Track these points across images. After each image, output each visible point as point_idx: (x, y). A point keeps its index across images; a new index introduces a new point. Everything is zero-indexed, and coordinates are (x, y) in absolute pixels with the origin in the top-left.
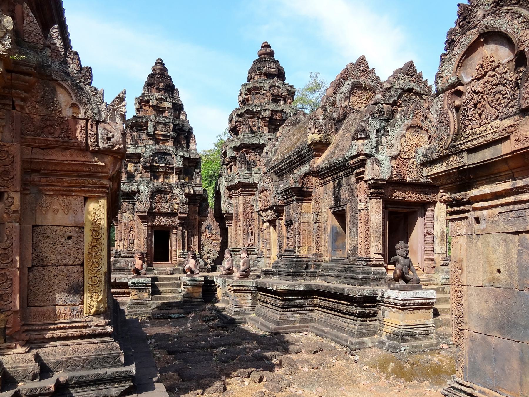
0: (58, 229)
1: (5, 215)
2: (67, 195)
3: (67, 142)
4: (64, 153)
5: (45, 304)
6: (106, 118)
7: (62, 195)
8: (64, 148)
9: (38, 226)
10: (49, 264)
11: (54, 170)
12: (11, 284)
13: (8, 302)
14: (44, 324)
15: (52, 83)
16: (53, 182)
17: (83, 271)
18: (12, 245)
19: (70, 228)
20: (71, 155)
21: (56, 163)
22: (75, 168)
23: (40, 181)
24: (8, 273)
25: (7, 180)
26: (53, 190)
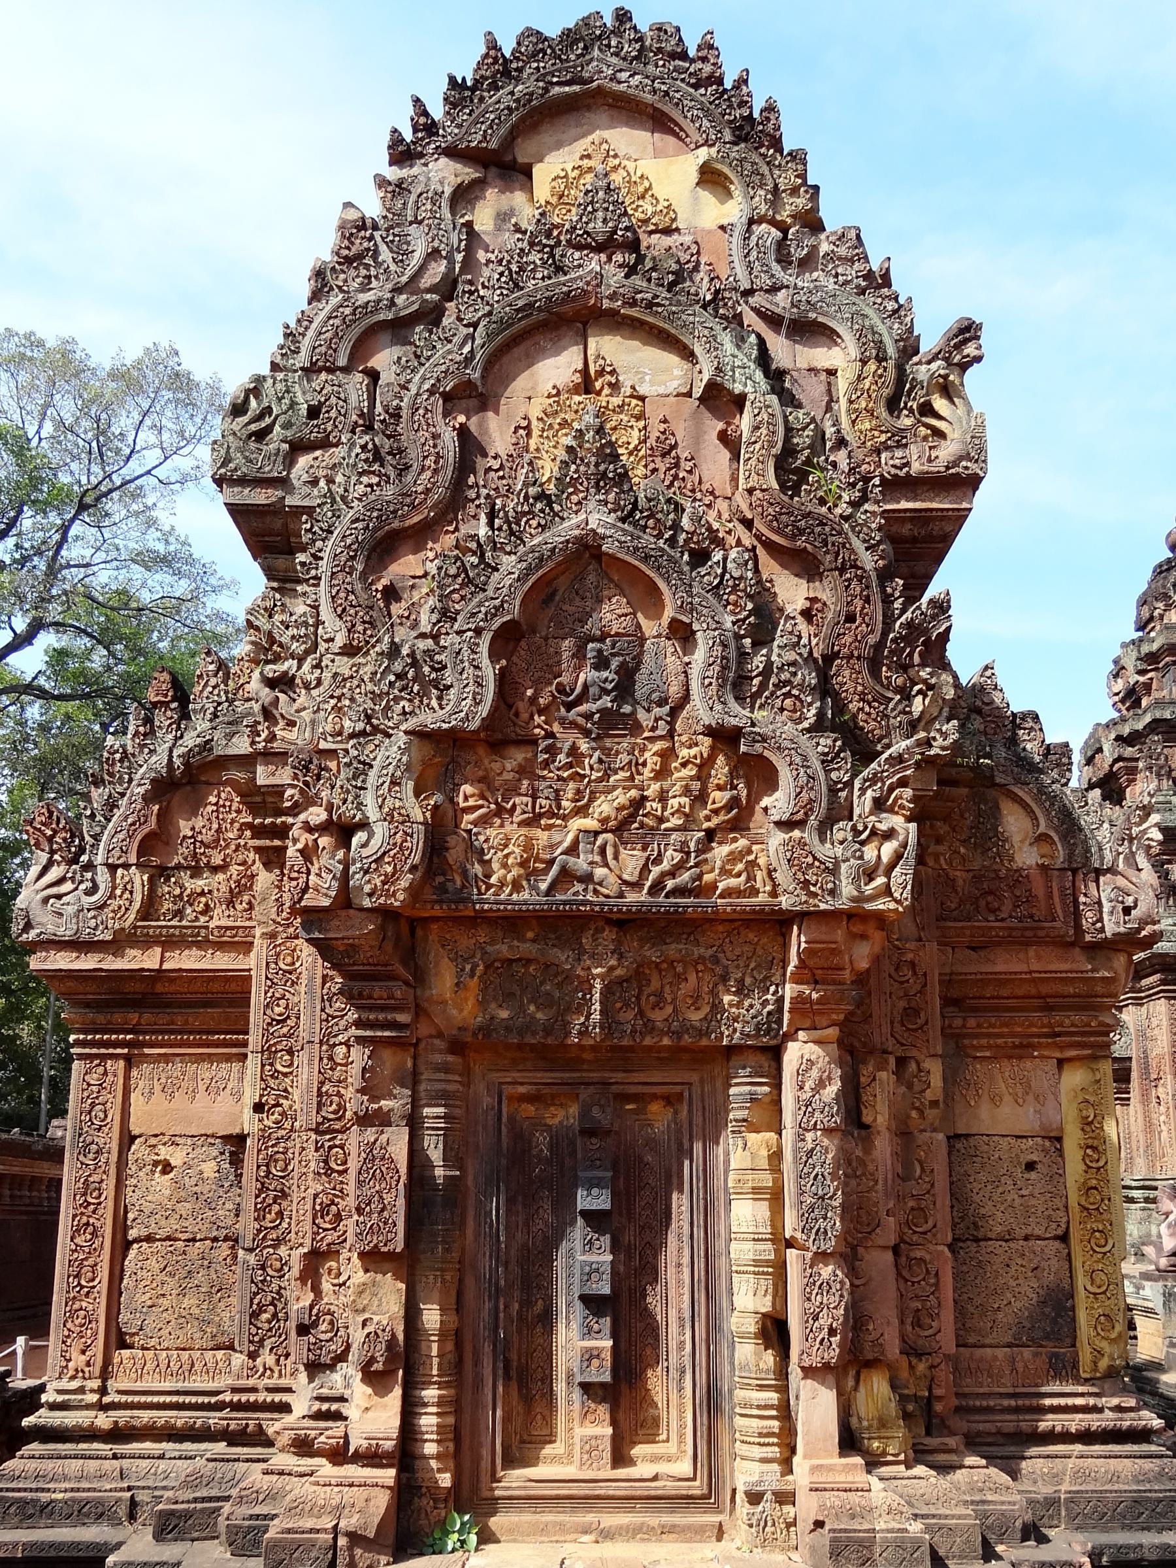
0: (1004, 1142)
1: (914, 1114)
2: (1020, 1058)
3: (1032, 929)
4: (1021, 956)
5: (987, 1341)
6: (1115, 860)
7: (1010, 1057)
8: (1021, 944)
9: (957, 1136)
10: (990, 1235)
11: (993, 998)
12: (937, 1285)
13: (931, 1332)
14: (989, 1395)
15: (993, 792)
16: (994, 1026)
17: (1069, 1254)
18: (933, 1185)
19: (1030, 1142)
20: (1039, 958)
21: (1002, 981)
22: (1044, 989)
23: (964, 1026)
24: (928, 1257)
25: (916, 1030)
26: (989, 1047)
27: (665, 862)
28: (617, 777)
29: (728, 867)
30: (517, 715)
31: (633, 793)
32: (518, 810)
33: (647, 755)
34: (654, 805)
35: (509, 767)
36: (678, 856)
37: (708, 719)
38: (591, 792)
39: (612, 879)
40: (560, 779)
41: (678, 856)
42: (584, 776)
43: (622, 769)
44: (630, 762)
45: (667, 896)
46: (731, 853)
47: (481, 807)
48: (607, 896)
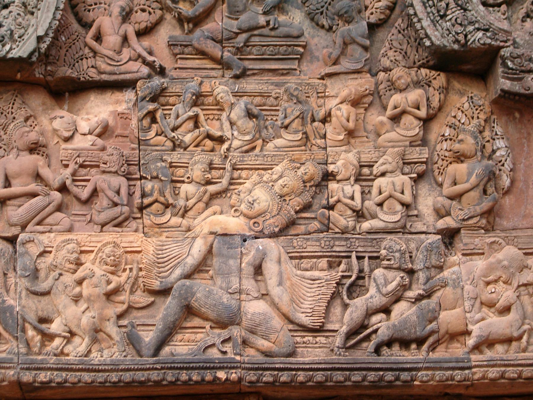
27: (373, 290)
28: (279, 142)
29: (486, 296)
30: (98, 38)
31: (310, 169)
32: (102, 202)
33: (331, 103)
34: (348, 189)
35: (84, 126)
36: (396, 279)
37: (438, 36)
38: (234, 168)
39: (277, 322)
40: (176, 145)
41: (396, 279)
42: (221, 140)
43: (286, 127)
44: (302, 117)
45: (377, 351)
46: (491, 269)
47: (34, 195)
48: (267, 354)
